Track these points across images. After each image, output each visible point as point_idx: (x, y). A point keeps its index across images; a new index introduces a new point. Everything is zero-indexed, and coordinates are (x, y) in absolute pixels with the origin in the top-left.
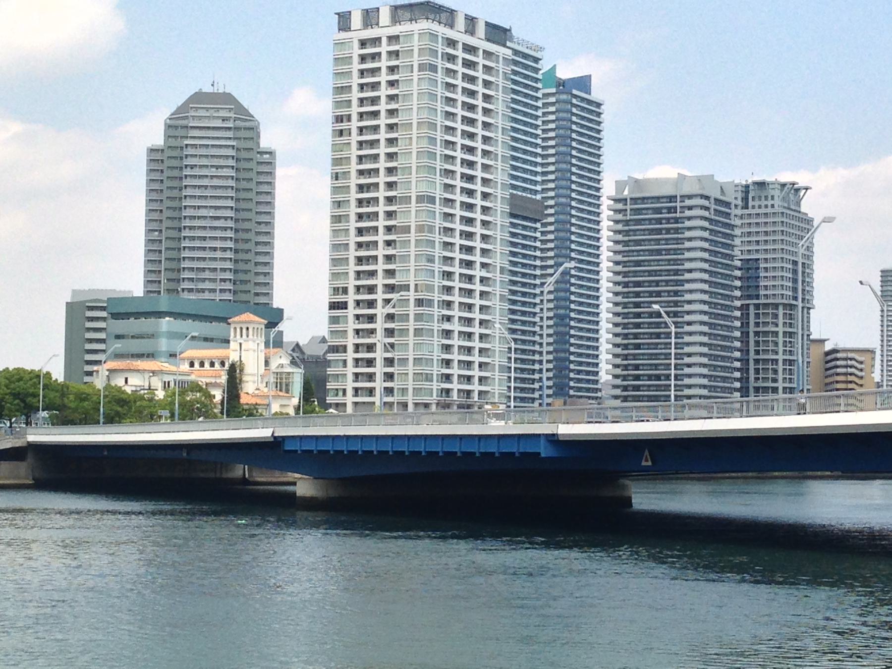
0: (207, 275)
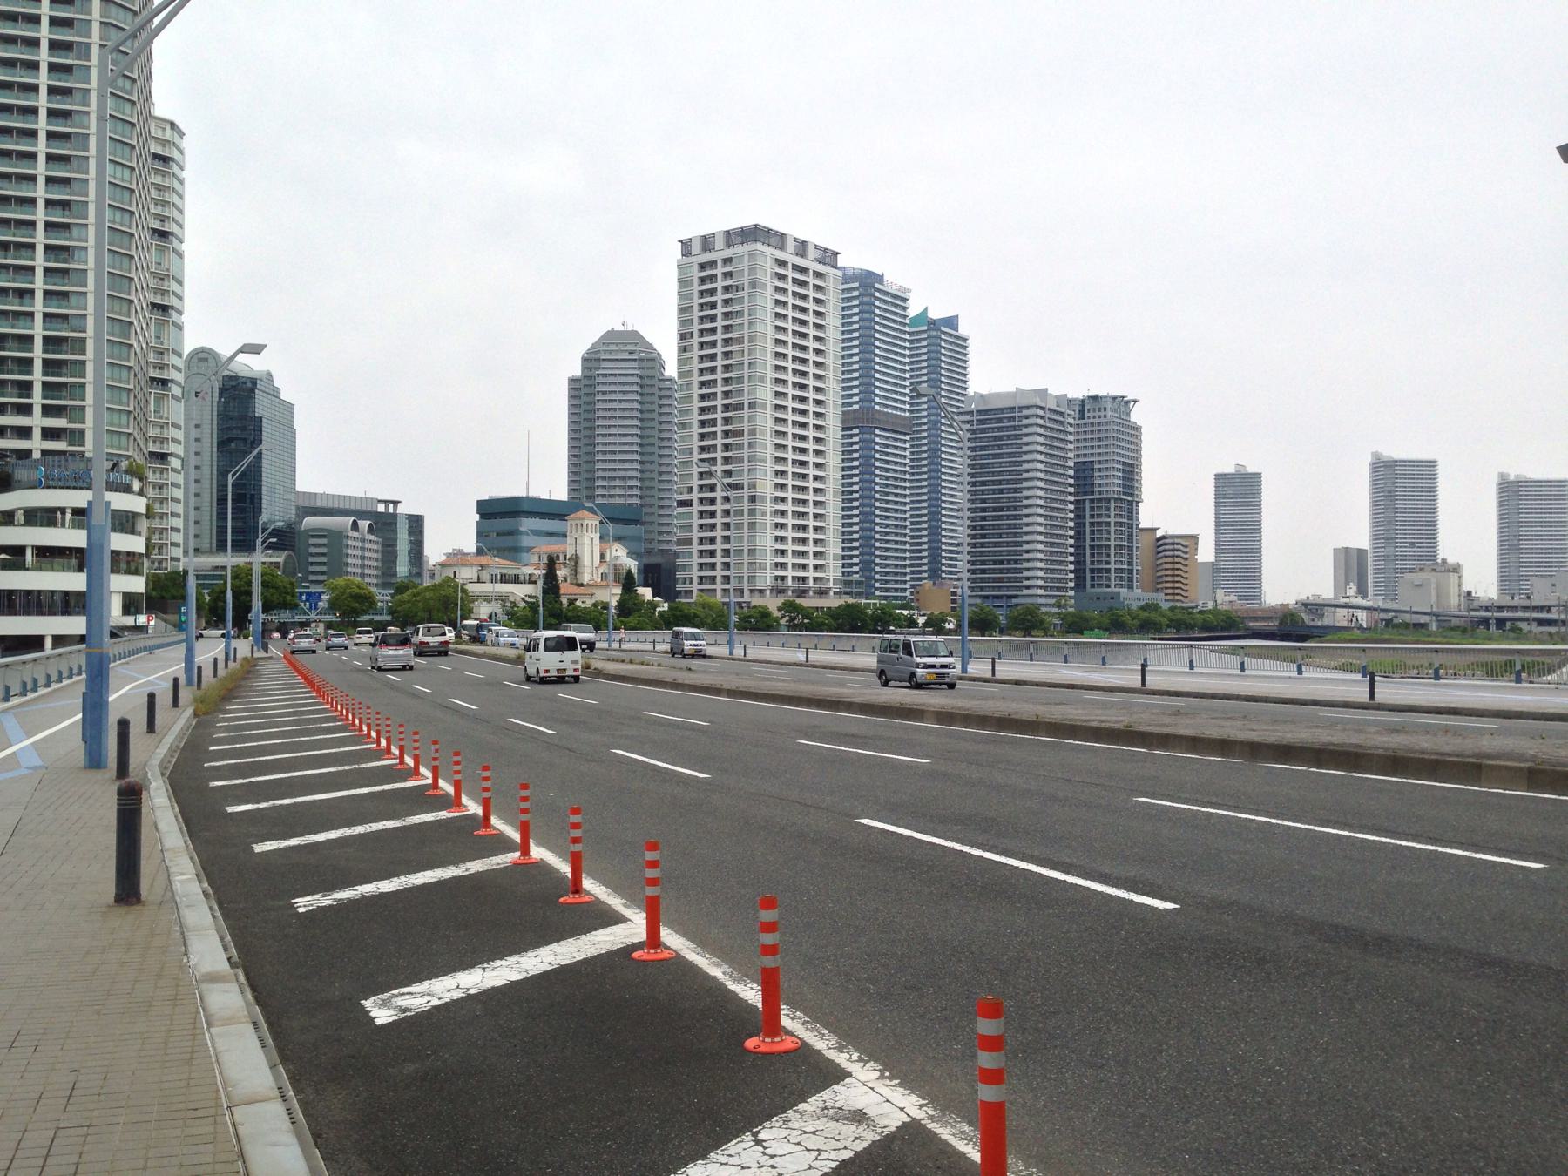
0: (618, 483)
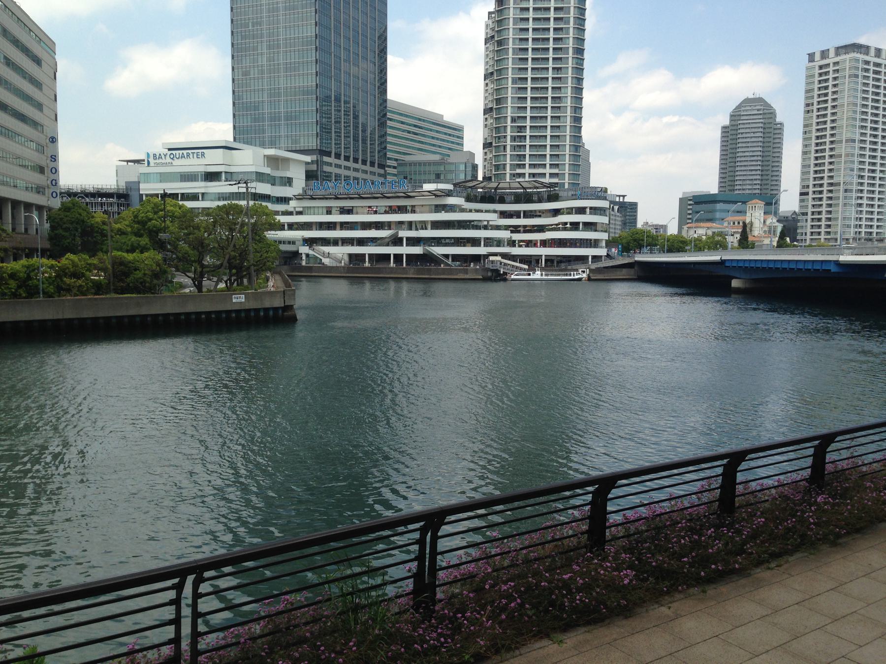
0: (748, 182)
